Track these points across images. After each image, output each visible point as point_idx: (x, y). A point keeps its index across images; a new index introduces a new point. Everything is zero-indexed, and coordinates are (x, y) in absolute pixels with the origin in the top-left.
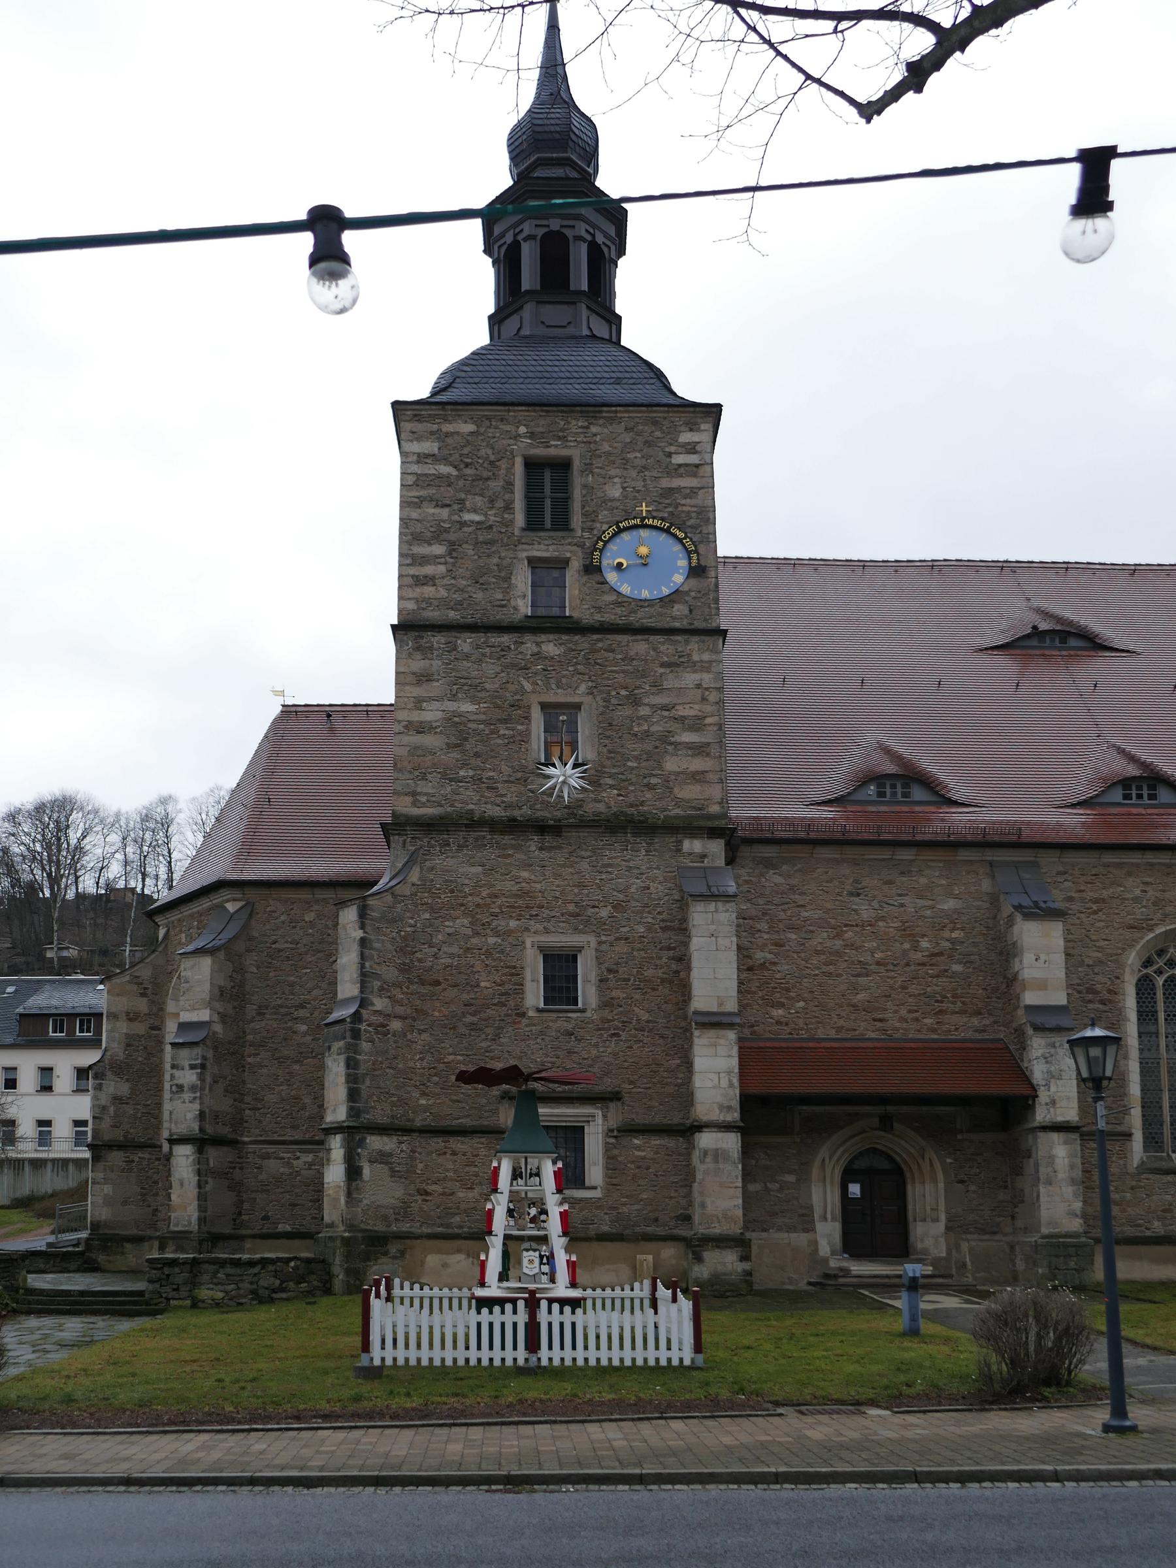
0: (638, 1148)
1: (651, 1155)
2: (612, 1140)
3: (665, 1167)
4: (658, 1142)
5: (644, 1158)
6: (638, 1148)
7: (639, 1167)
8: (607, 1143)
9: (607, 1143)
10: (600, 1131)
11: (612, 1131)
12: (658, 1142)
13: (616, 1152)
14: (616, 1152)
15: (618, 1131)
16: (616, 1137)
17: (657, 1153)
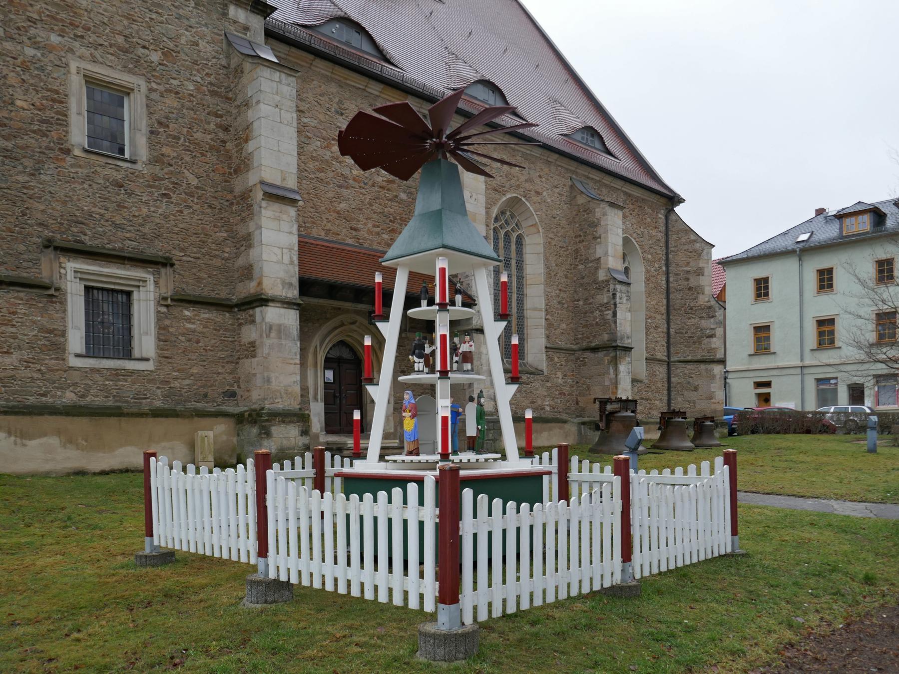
0: (189, 320)
1: (200, 329)
2: (164, 309)
3: (213, 341)
4: (207, 316)
5: (194, 331)
6: (189, 320)
7: (189, 340)
8: (159, 312)
9: (159, 312)
10: (152, 298)
11: (165, 299)
12: (207, 316)
13: (167, 322)
14: (167, 322)
15: (172, 300)
16: (167, 306)
17: (205, 327)
